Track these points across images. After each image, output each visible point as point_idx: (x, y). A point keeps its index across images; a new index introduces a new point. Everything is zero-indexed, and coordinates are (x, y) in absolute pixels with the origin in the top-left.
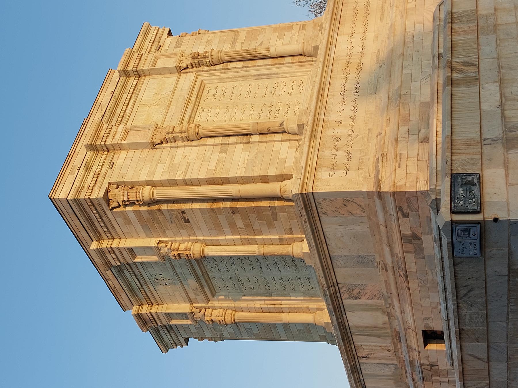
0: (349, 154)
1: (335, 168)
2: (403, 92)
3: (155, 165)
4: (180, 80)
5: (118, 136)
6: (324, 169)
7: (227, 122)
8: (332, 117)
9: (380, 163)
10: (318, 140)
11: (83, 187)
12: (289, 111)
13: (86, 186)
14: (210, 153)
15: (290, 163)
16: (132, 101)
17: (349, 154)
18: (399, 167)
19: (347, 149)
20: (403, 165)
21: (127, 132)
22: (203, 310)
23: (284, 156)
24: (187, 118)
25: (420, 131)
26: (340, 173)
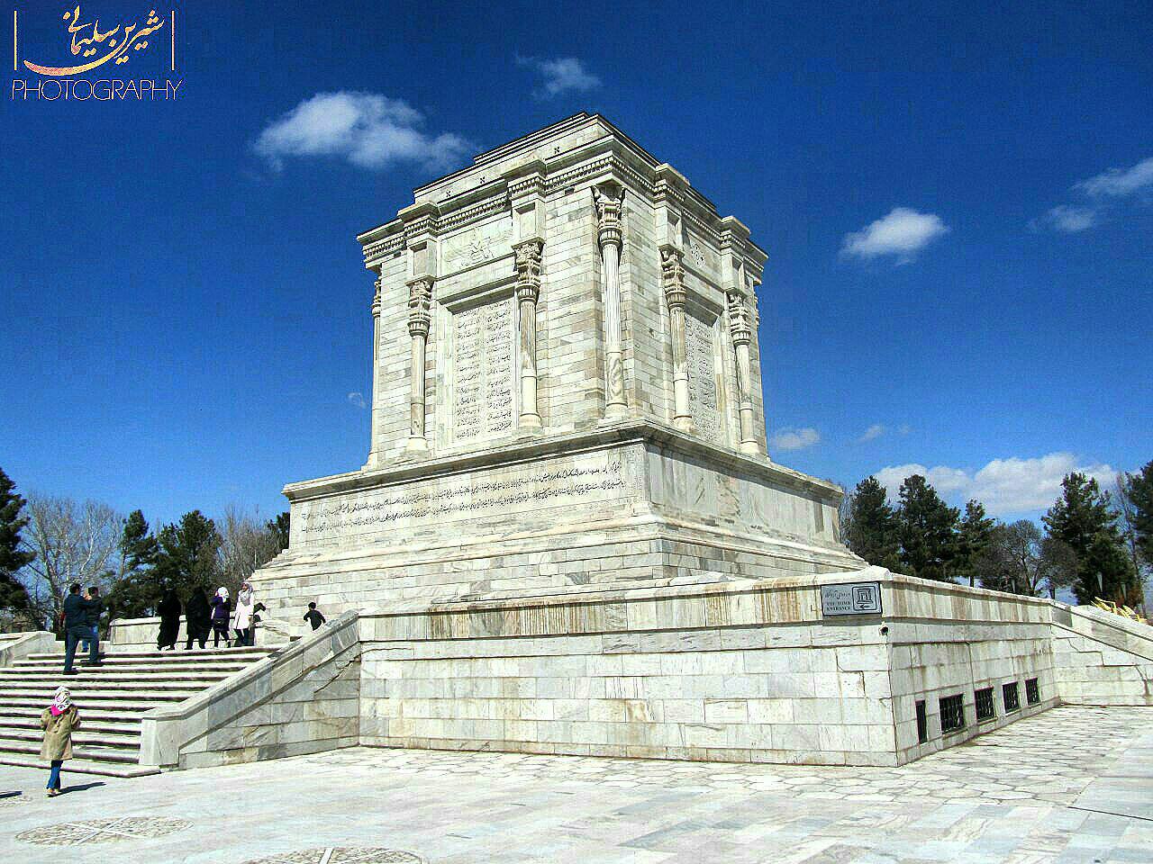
0: (321, 529)
7: (457, 353)
8: (360, 498)
17: (321, 529)
21: (424, 246)
25: (291, 598)
26: (305, 523)
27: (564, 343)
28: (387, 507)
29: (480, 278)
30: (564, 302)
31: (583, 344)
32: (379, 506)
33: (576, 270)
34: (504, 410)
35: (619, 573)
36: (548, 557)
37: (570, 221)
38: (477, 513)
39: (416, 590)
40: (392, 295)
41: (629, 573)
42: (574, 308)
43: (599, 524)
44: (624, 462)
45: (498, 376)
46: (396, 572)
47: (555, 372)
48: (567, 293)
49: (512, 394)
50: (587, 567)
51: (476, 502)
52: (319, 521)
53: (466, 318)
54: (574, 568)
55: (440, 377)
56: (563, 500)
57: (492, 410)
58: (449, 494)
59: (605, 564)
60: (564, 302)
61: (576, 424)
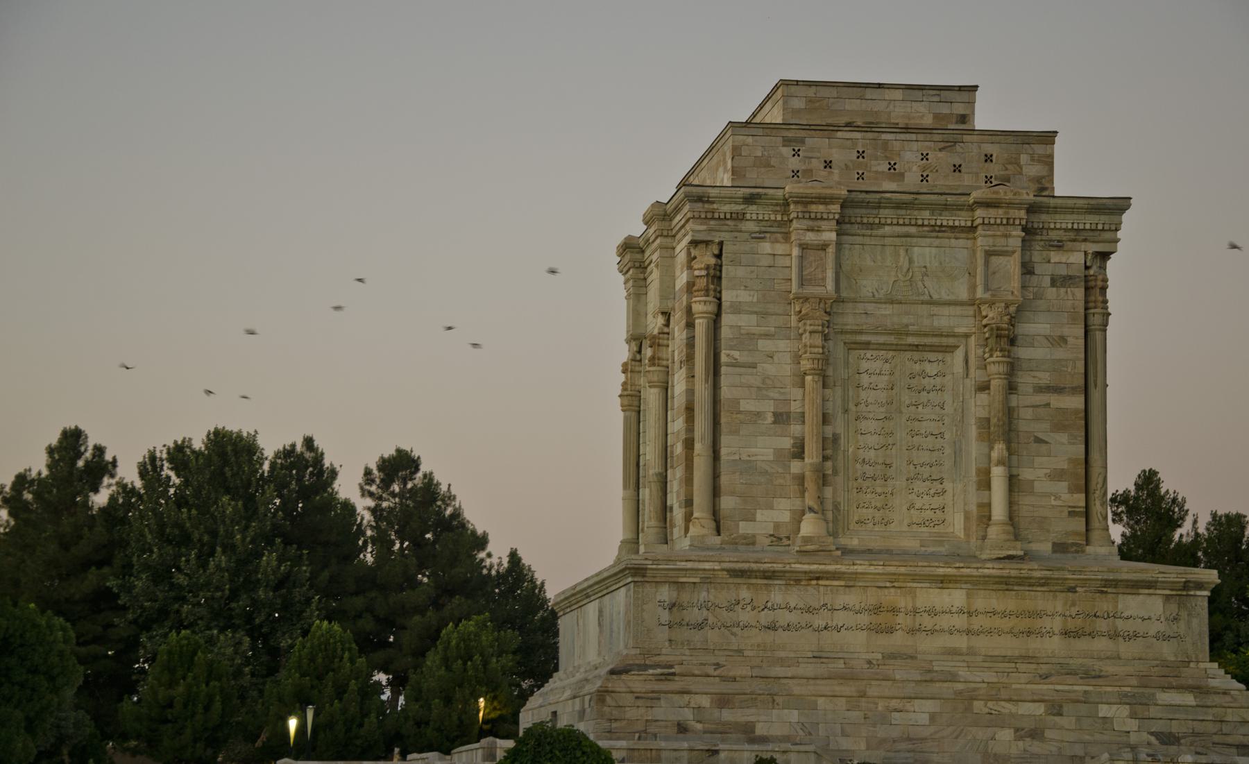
0: (700, 626)
1: (675, 609)
2: (779, 699)
3: (755, 309)
4: (959, 308)
5: (810, 237)
6: (675, 594)
8: (777, 597)
9: (659, 671)
10: (731, 580)
11: (713, 203)
12: (871, 510)
13: (715, 206)
14: (777, 396)
15: (745, 528)
16: (913, 230)
17: (700, 626)
18: (637, 698)
19: (710, 622)
20: (640, 702)
21: (823, 247)
22: (638, 357)
23: (759, 516)
24: (864, 338)
25: (698, 722)
26: (665, 616)
27: (1039, 441)
28: (824, 613)
29: (905, 320)
30: (1040, 389)
31: (1067, 449)
32: (809, 610)
33: (1060, 353)
34: (936, 502)
35: (1216, 739)
36: (1125, 711)
37: (1054, 283)
38: (981, 643)
39: (932, 729)
40: (744, 296)
41: (1230, 740)
42: (1057, 401)
43: (1174, 682)
44: (1184, 614)
45: (925, 457)
46: (894, 703)
47: (1026, 474)
48: (1045, 378)
49: (948, 485)
50: (1175, 728)
51: (976, 627)
52: (695, 615)
53: (871, 364)
54: (1157, 727)
55: (836, 438)
56: (1101, 644)
57: (913, 496)
58: (932, 612)
59: (1199, 727)
60: (1040, 389)
61: (1054, 544)
